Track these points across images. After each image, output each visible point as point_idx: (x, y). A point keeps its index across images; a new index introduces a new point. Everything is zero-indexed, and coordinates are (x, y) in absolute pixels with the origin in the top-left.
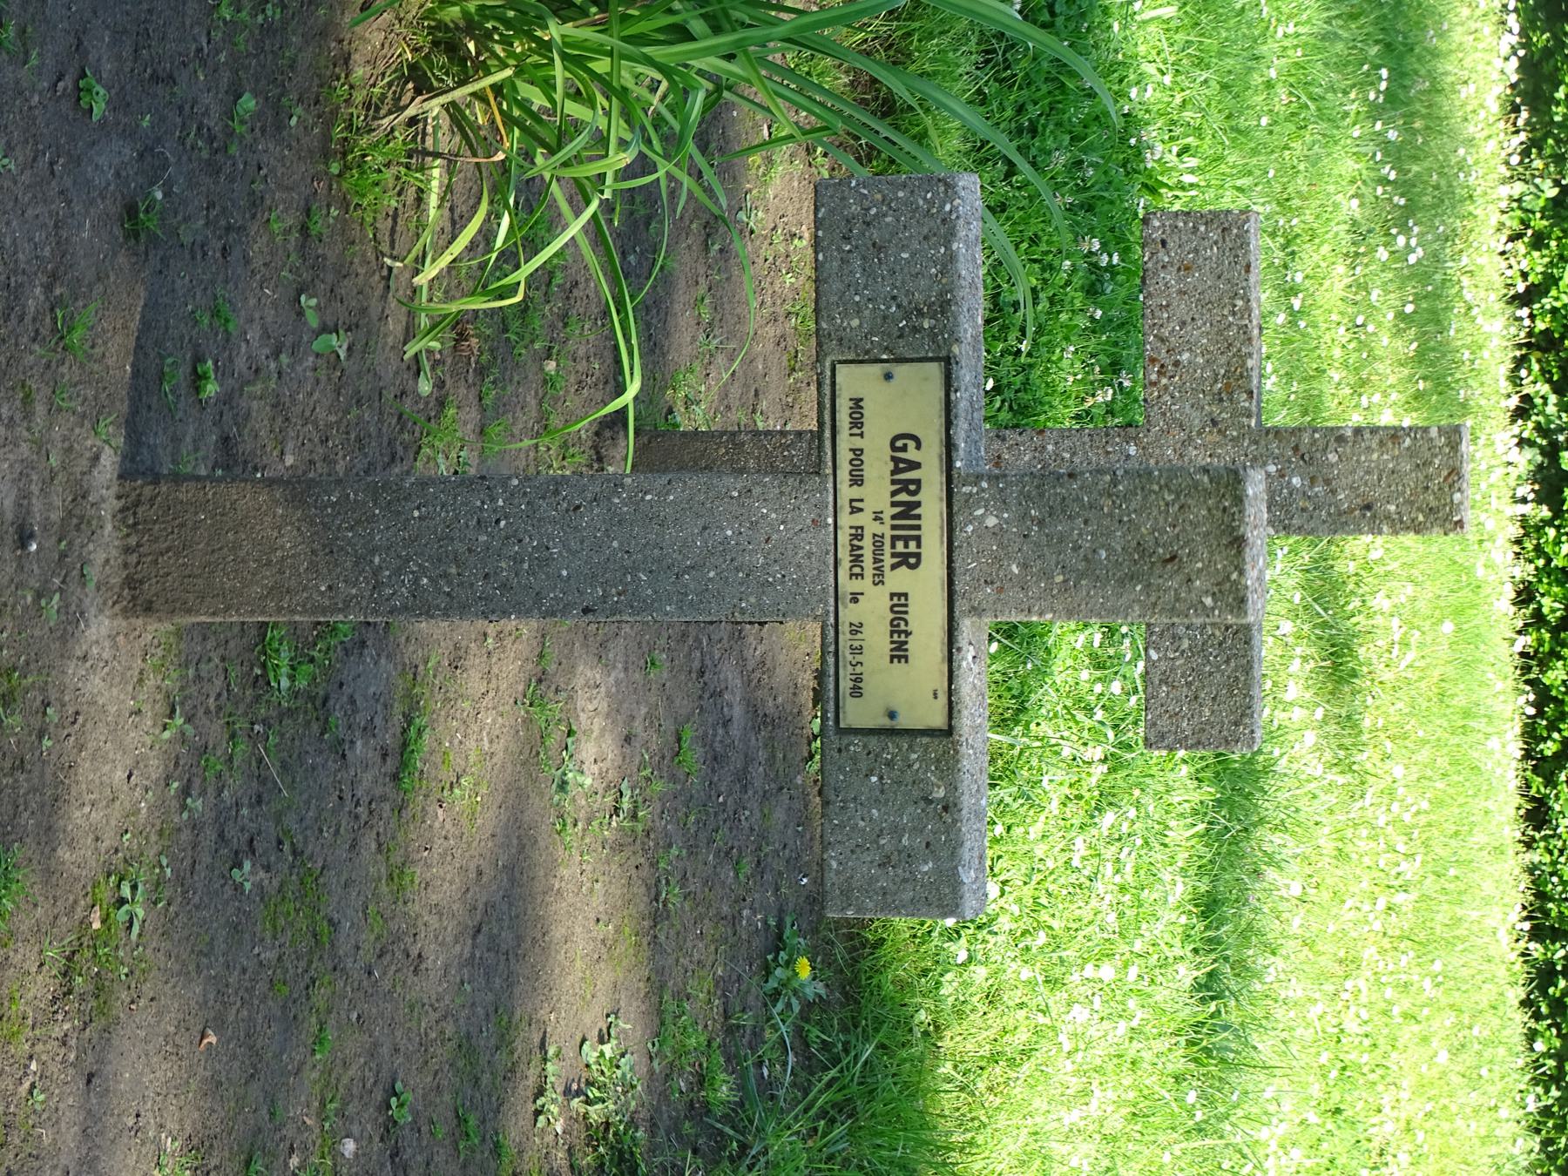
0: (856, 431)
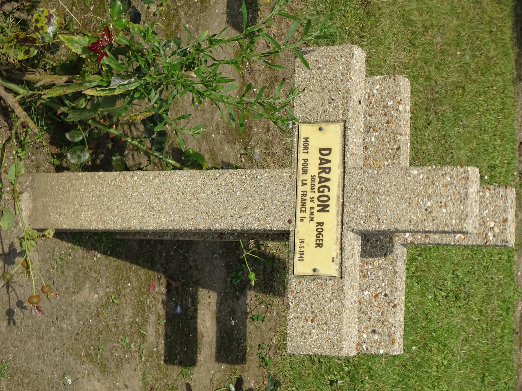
0: (305, 151)
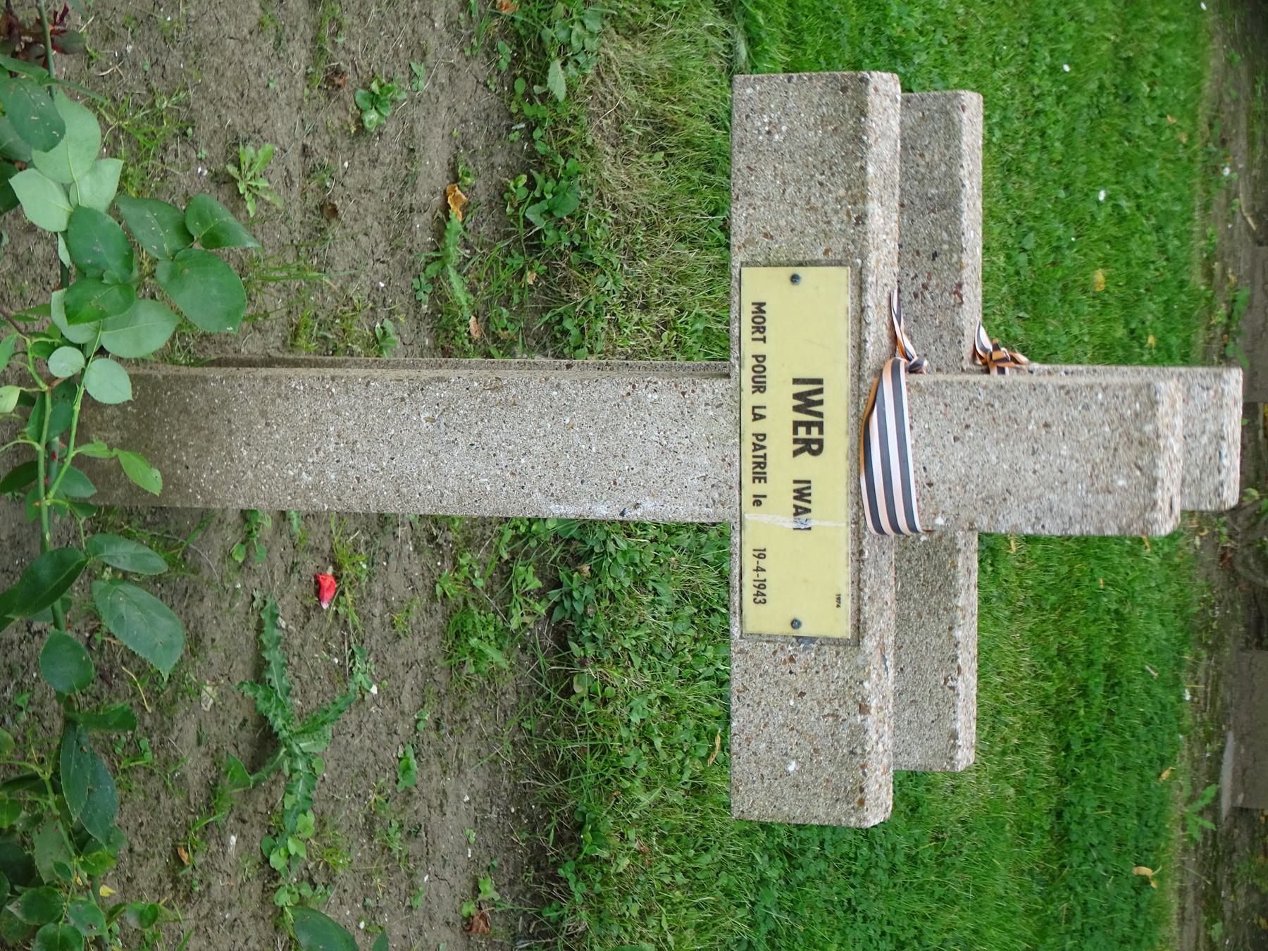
0: (758, 335)
